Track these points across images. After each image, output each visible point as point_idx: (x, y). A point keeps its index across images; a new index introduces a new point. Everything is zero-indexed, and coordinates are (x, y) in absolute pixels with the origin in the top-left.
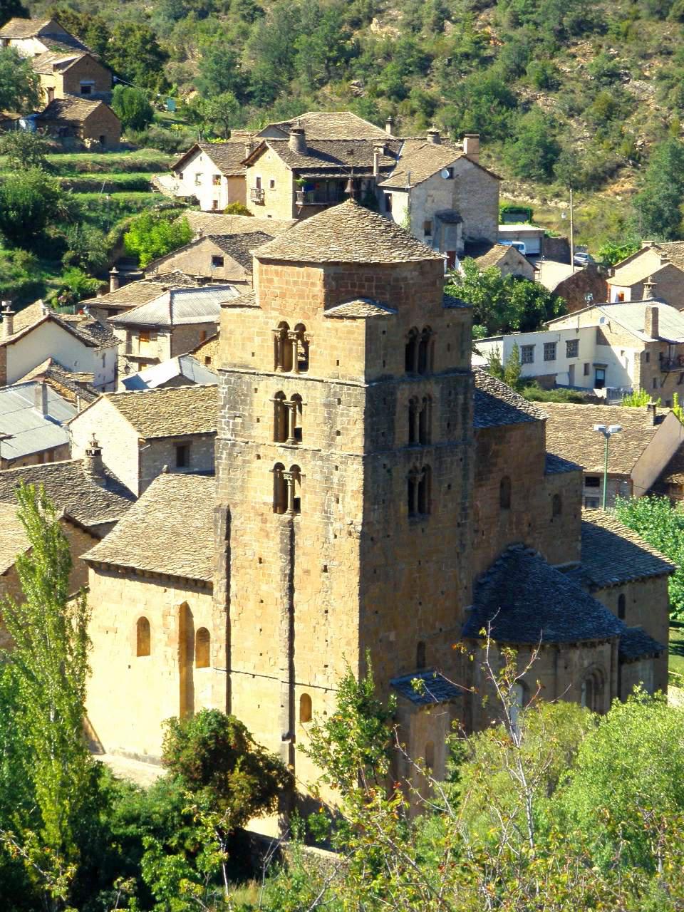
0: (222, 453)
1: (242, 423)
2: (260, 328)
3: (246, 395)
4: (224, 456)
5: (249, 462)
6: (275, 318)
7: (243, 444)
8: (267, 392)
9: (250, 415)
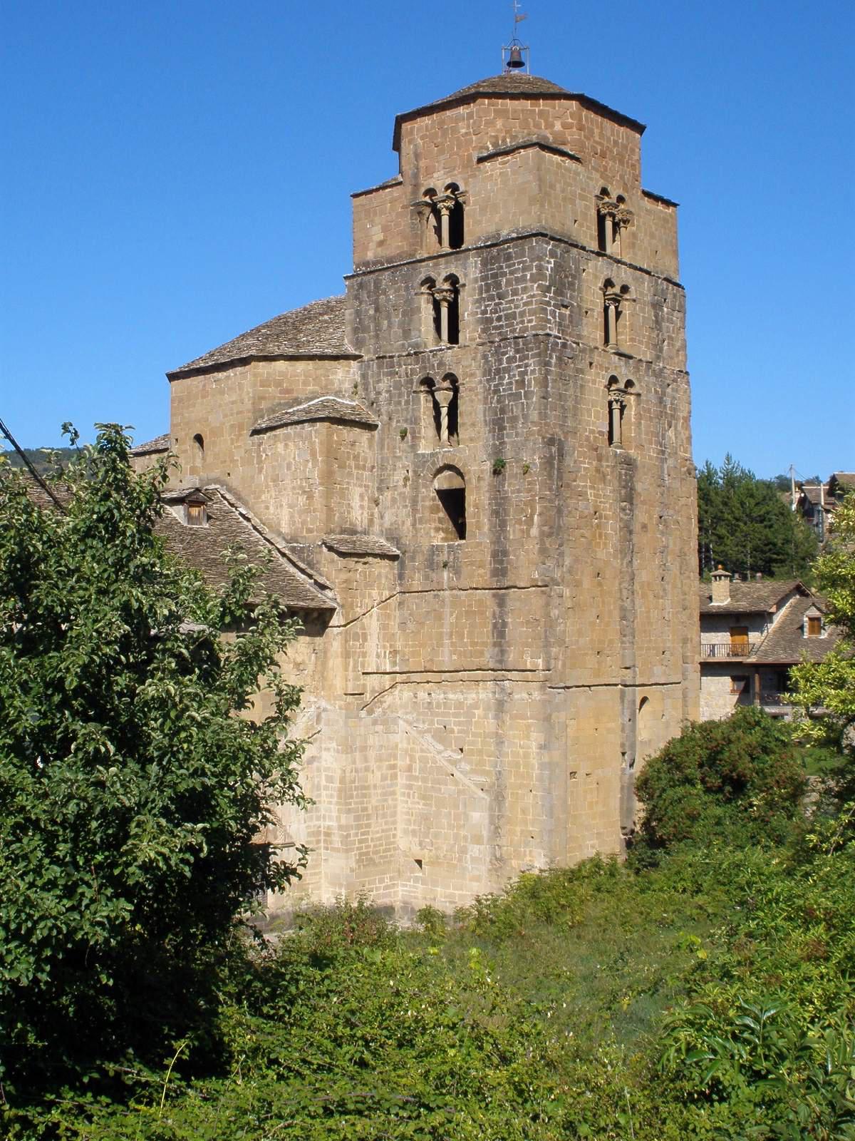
0: (551, 358)
1: (570, 316)
4: (553, 361)
9: (578, 306)
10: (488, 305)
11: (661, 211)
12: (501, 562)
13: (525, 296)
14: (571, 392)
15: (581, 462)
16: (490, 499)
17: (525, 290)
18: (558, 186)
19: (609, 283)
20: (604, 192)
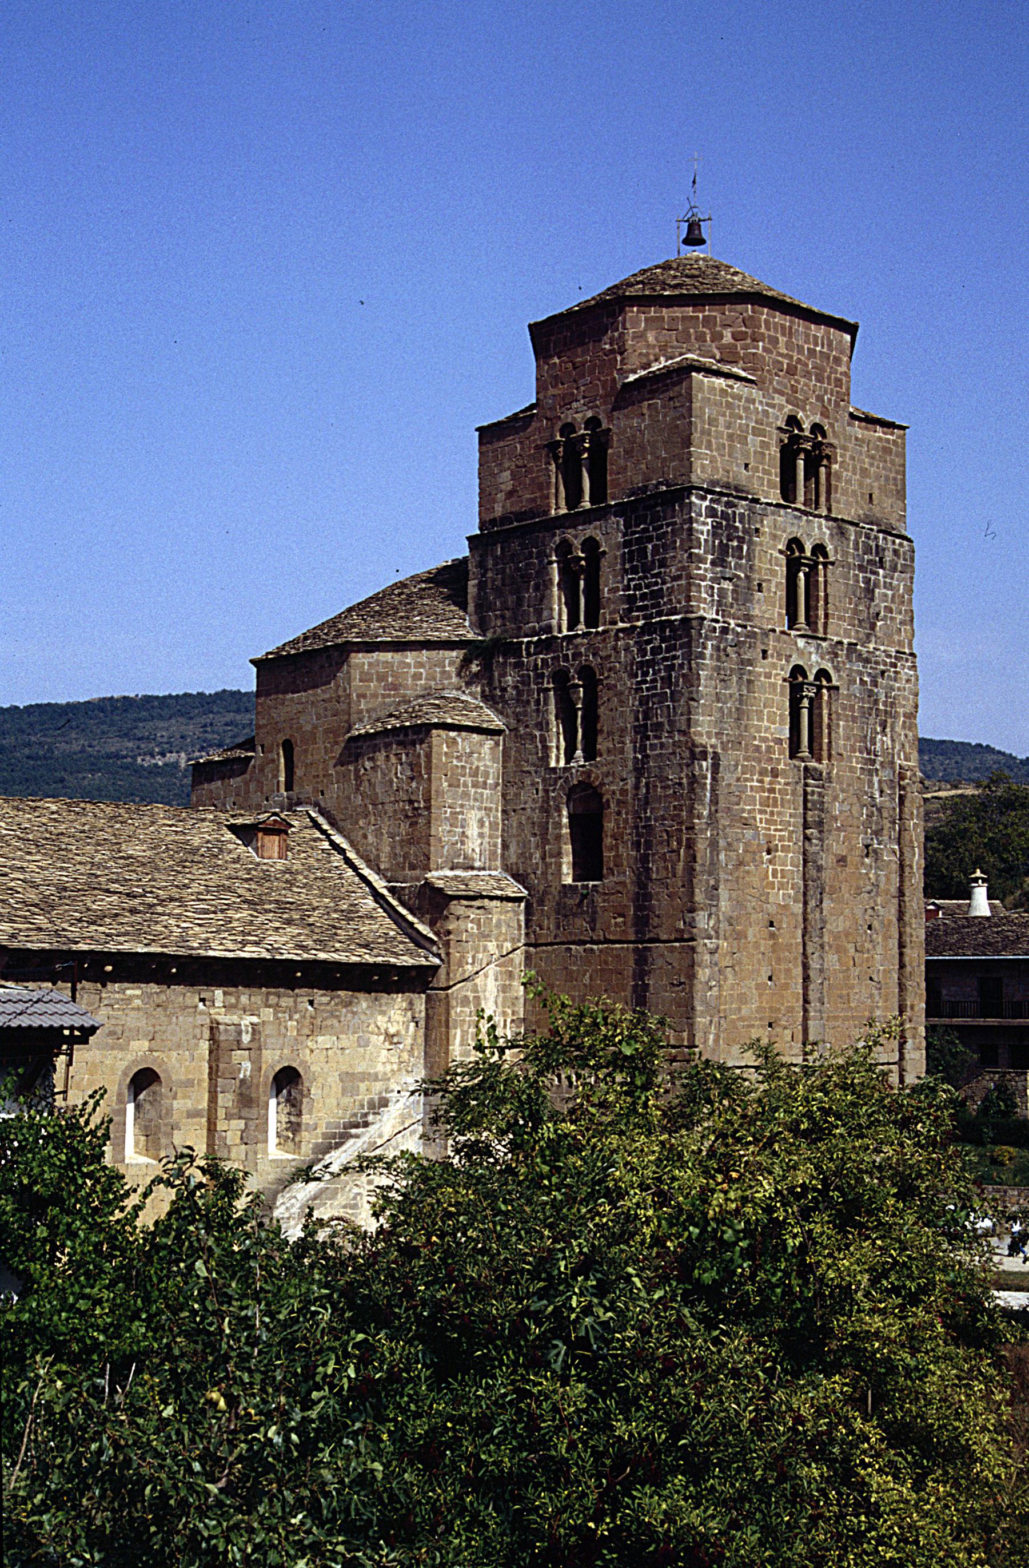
0: (705, 648)
2: (756, 422)
3: (741, 540)
4: (708, 652)
5: (750, 662)
6: (781, 407)
7: (739, 629)
8: (774, 537)
10: (633, 579)
11: (880, 439)
14: (733, 690)
15: (746, 780)
18: (721, 419)
19: (795, 543)
20: (793, 421)
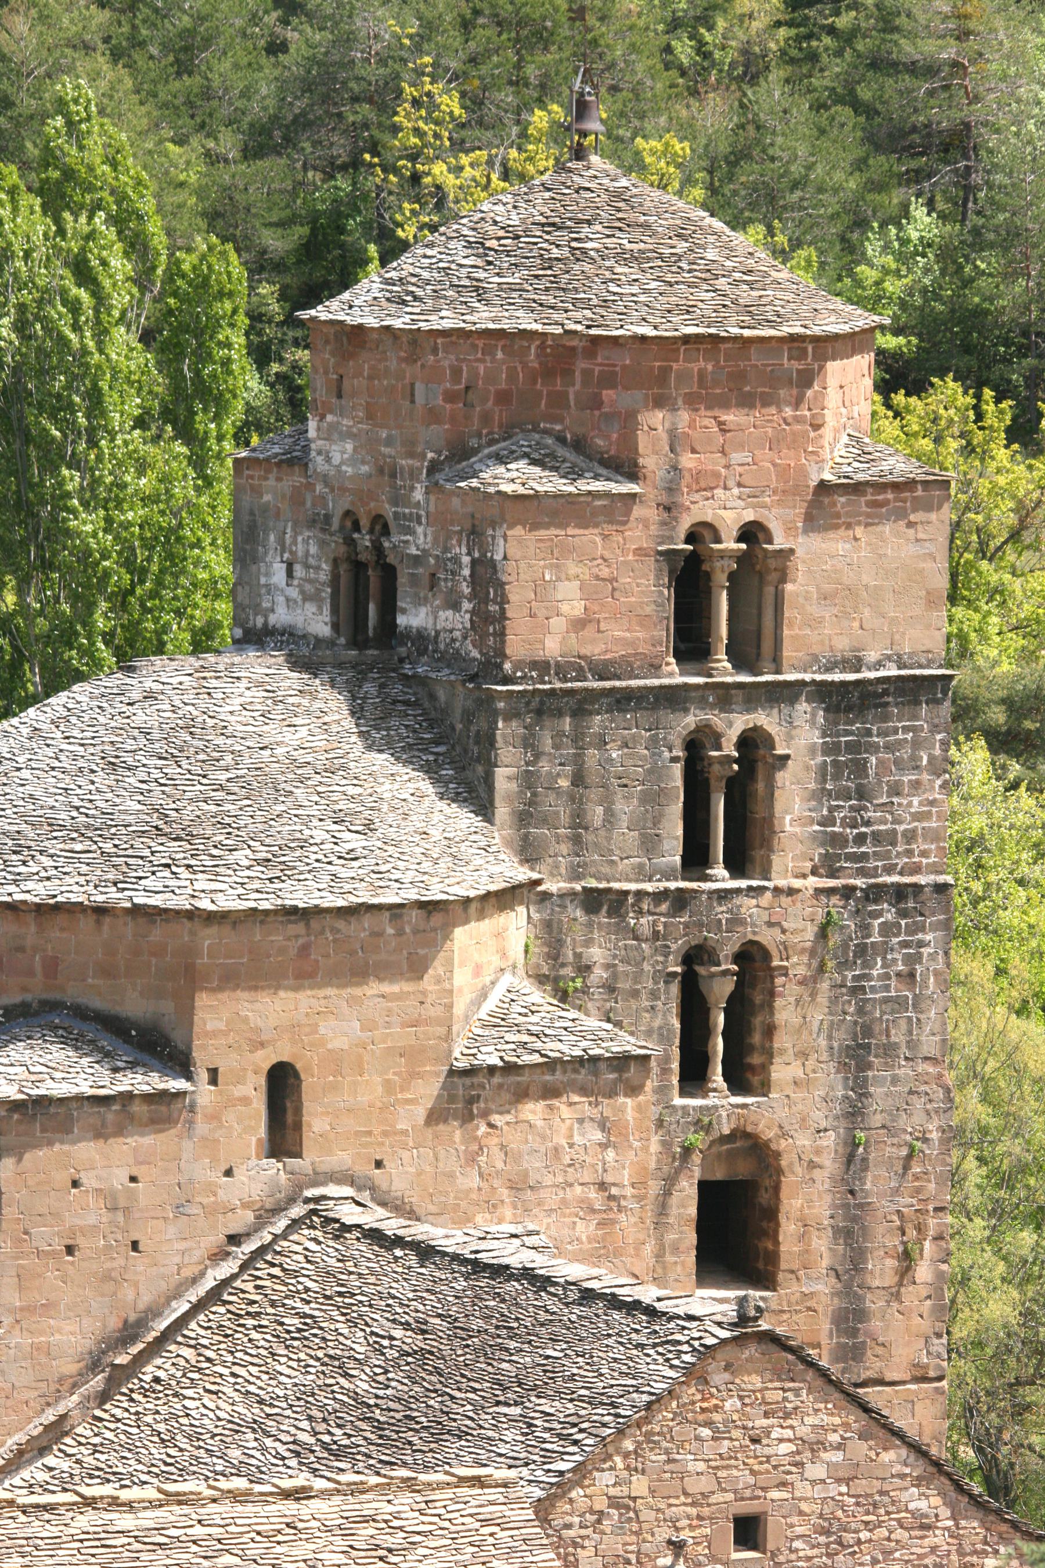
12: (854, 1333)
13: (916, 801)
16: (834, 1206)
17: (916, 785)
